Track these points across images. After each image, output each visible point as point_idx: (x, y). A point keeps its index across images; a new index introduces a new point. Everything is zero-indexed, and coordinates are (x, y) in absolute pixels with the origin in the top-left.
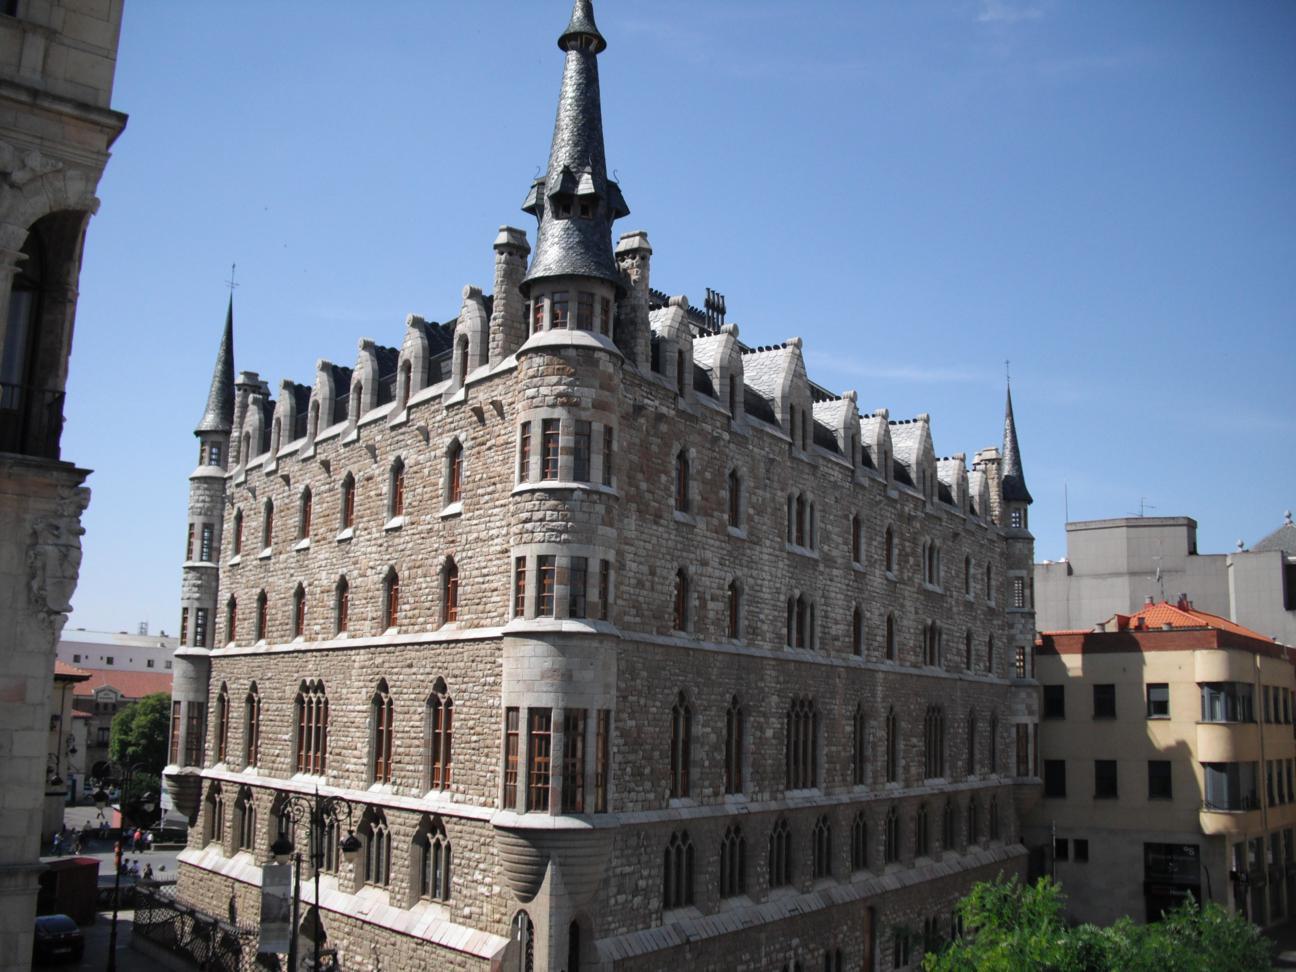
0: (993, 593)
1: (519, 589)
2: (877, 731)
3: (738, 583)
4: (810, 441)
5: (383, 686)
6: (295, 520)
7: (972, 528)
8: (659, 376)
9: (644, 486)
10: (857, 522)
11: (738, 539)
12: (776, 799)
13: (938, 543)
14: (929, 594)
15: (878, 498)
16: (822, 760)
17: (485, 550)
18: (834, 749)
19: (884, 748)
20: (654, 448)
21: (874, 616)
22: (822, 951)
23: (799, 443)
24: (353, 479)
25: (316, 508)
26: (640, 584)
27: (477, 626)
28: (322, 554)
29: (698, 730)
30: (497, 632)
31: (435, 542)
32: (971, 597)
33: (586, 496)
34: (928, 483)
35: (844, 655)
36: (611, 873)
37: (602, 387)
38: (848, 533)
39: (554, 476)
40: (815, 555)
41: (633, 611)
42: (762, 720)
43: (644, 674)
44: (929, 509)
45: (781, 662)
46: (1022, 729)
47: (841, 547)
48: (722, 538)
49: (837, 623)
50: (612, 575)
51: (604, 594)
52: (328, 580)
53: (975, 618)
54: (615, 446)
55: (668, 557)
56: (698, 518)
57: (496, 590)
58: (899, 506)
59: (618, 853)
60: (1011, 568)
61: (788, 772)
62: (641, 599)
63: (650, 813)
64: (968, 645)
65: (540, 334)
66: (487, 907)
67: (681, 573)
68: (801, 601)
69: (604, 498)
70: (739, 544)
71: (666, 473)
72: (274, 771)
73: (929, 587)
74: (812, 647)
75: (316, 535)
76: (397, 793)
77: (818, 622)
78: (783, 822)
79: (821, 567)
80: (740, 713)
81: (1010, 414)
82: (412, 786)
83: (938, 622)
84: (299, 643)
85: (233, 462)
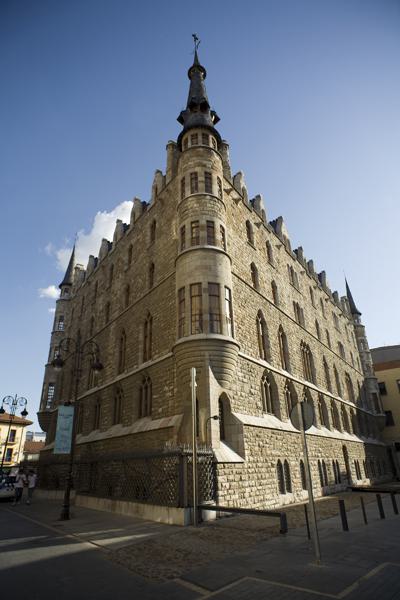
46: (374, 394)
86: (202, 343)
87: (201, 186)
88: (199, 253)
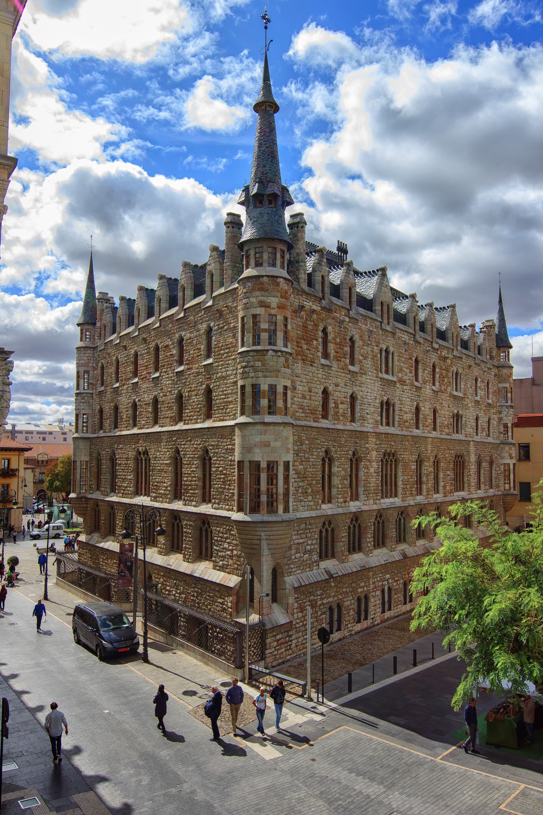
0: (491, 396)
1: (243, 401)
2: (428, 468)
3: (354, 395)
4: (391, 320)
5: (178, 451)
6: (131, 368)
7: (479, 362)
8: (313, 290)
9: (305, 347)
10: (417, 361)
11: (354, 372)
12: (376, 504)
13: (460, 371)
14: (455, 397)
15: (428, 348)
16: (400, 483)
17: (225, 381)
18: (406, 477)
19: (432, 477)
20: (310, 327)
21: (426, 409)
22: (402, 581)
23: (386, 321)
25: (140, 362)
26: (304, 397)
27: (223, 420)
29: (335, 469)
30: (232, 423)
31: (201, 378)
32: (478, 398)
33: (274, 354)
34: (455, 339)
35: (410, 429)
36: (292, 543)
37: (281, 297)
38: (412, 367)
39: (259, 344)
40: (395, 379)
41: (301, 411)
42: (368, 463)
43: (307, 442)
44: (455, 353)
45: (378, 435)
47: (408, 374)
48: (346, 372)
49: (406, 413)
50: (289, 393)
51: (285, 401)
52: (148, 398)
53: (480, 409)
54: (289, 327)
55: (318, 383)
56: (334, 362)
57: (232, 402)
58: (439, 352)
59: (296, 532)
60: (500, 383)
61: (382, 490)
62: (305, 404)
63: (311, 512)
64: (477, 423)
65: (249, 270)
66: (231, 562)
67: (325, 392)
68: (388, 403)
69: (284, 353)
70: (355, 375)
71: (316, 340)
72: (124, 495)
73: (455, 393)
74: (393, 426)
76: (185, 505)
77: (397, 413)
78: (380, 514)
79: (398, 385)
80: (356, 460)
81: (500, 302)
82: (193, 501)
83: (460, 412)
84: (135, 431)
86: (259, 525)
87: (264, 336)
88: (259, 427)
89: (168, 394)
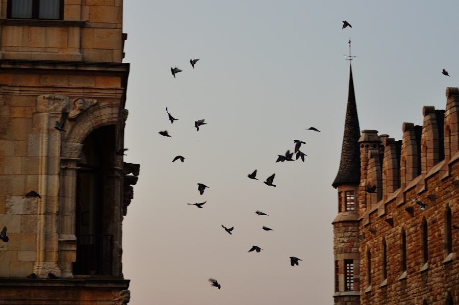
6: (398, 256)
24: (426, 221)
25: (409, 246)
28: (414, 285)
75: (410, 268)
85: (363, 207)
89: (438, 297)
